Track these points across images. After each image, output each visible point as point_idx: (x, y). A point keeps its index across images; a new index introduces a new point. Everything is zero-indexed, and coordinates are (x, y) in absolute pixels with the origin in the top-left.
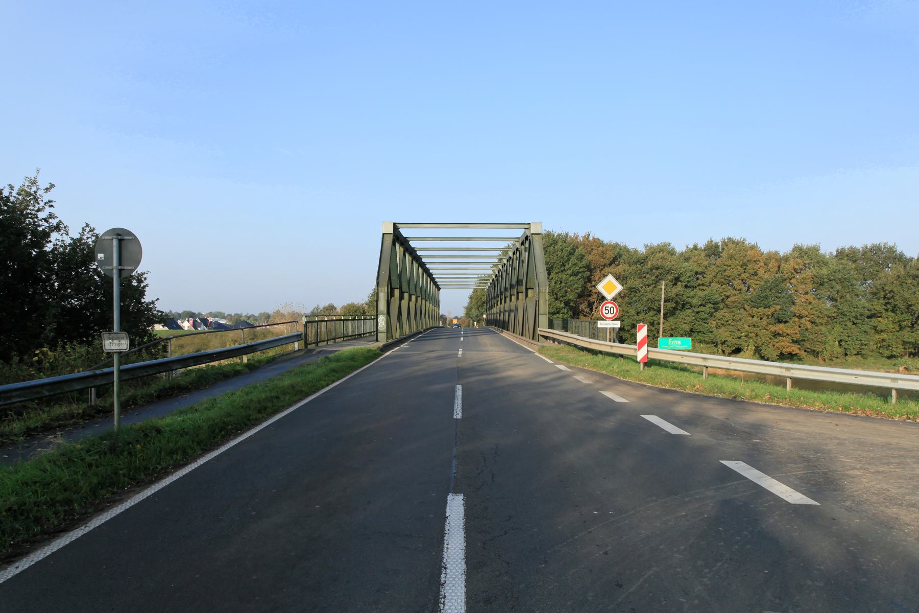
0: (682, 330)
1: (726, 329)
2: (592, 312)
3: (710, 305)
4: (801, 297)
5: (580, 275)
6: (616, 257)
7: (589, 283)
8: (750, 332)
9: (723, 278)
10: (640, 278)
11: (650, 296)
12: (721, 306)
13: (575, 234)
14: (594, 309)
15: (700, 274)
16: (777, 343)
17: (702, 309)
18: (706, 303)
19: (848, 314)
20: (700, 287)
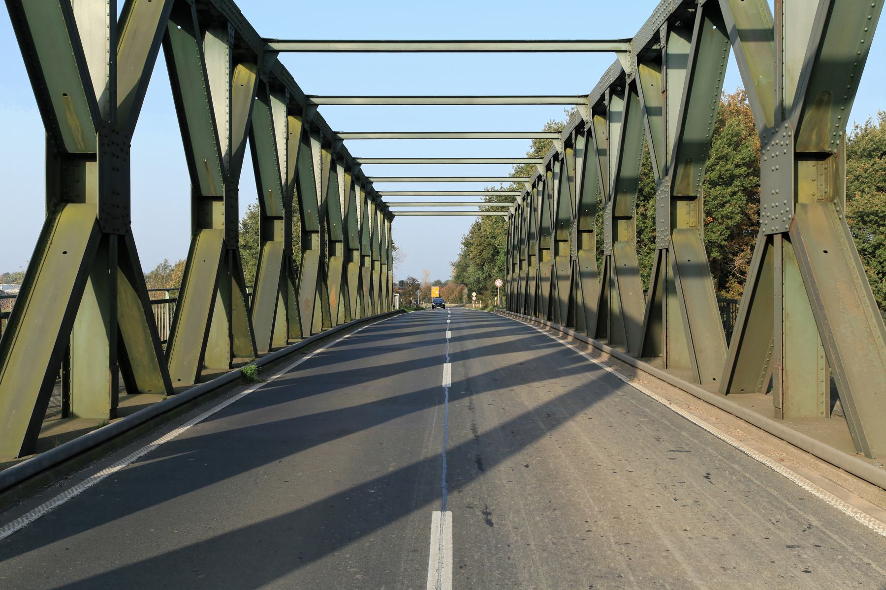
5: (737, 182)
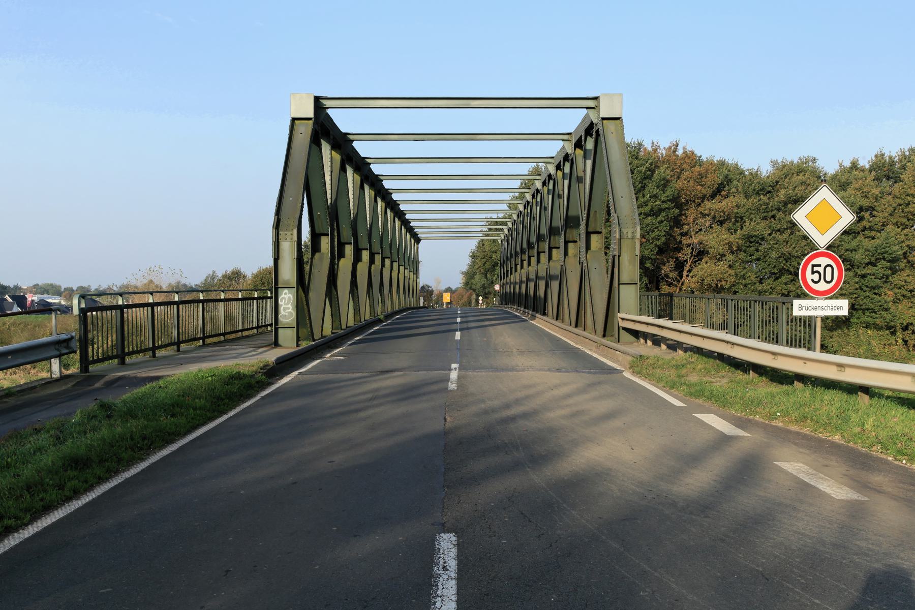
1: (910, 305)
2: (681, 277)
3: (883, 263)
5: (663, 214)
6: (722, 184)
7: (677, 228)
9: (904, 217)
10: (765, 218)
11: (785, 249)
12: (902, 265)
13: (653, 143)
14: (685, 273)
15: (867, 210)
17: (870, 270)
18: (878, 259)
20: (866, 233)
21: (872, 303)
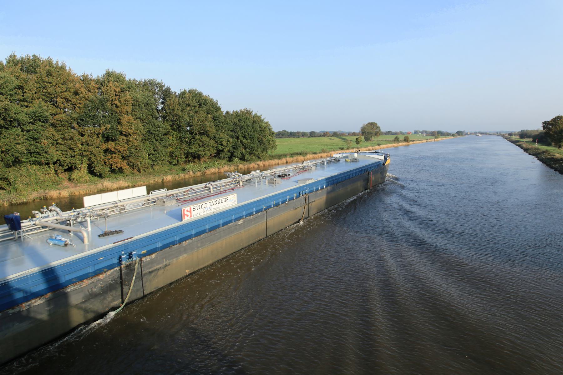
0: (18, 152)
4: (125, 117)
8: (84, 151)
16: (108, 159)
17: (31, 127)
19: (154, 132)
21: (36, 148)
